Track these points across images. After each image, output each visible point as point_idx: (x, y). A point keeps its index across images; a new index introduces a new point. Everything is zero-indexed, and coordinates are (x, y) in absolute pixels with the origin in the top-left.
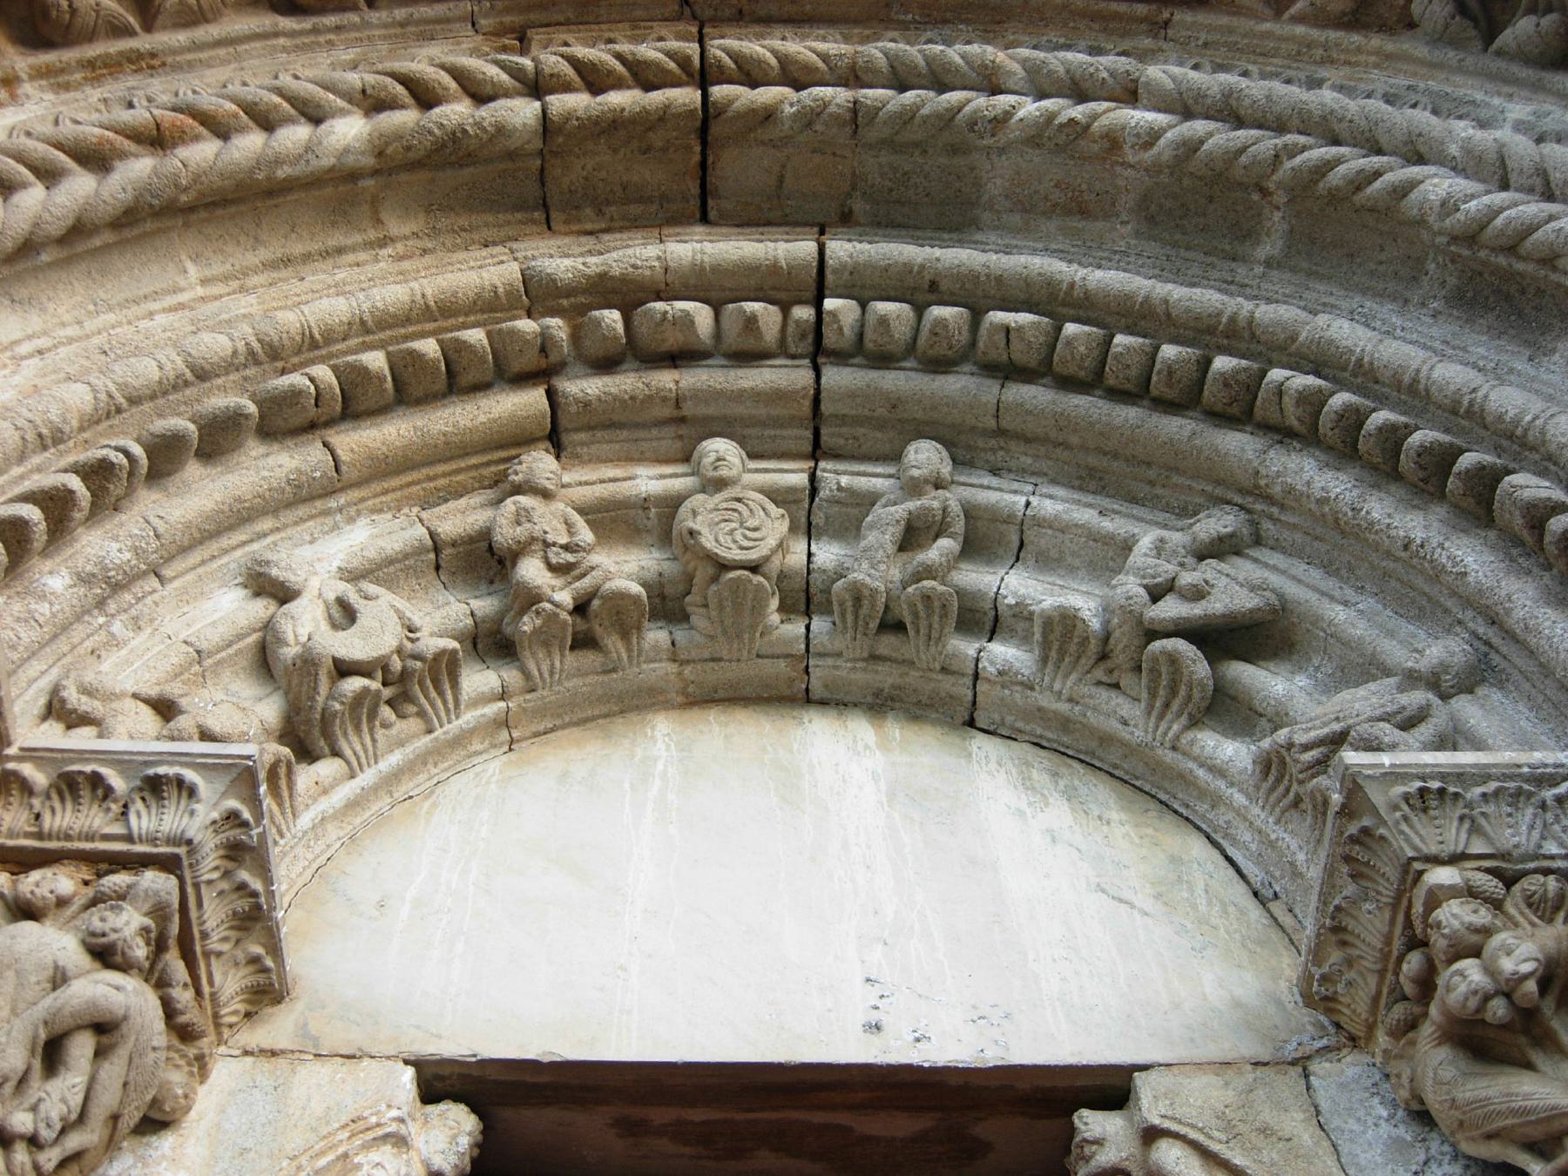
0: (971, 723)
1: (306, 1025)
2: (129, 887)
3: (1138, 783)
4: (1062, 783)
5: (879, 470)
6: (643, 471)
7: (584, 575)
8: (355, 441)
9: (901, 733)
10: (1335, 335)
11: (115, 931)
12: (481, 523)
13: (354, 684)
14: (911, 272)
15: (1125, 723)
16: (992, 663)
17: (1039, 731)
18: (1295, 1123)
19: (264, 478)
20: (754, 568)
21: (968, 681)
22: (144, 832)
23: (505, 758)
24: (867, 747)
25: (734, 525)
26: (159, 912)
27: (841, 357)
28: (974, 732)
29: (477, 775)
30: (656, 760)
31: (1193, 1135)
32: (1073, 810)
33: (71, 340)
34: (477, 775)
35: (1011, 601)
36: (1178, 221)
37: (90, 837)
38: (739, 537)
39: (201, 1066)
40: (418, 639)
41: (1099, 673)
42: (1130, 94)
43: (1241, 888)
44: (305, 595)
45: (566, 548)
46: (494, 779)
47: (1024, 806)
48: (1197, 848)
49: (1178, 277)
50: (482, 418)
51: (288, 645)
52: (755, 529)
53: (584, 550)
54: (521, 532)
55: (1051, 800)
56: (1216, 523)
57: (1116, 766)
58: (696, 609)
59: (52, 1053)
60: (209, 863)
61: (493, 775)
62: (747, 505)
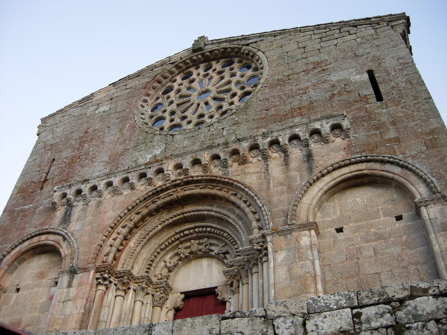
6: (188, 243)
8: (168, 249)
13: (172, 268)
18: (225, 289)
26: (164, 290)
39: (169, 296)
42: (212, 211)
49: (219, 225)
59: (160, 299)
60: (165, 286)
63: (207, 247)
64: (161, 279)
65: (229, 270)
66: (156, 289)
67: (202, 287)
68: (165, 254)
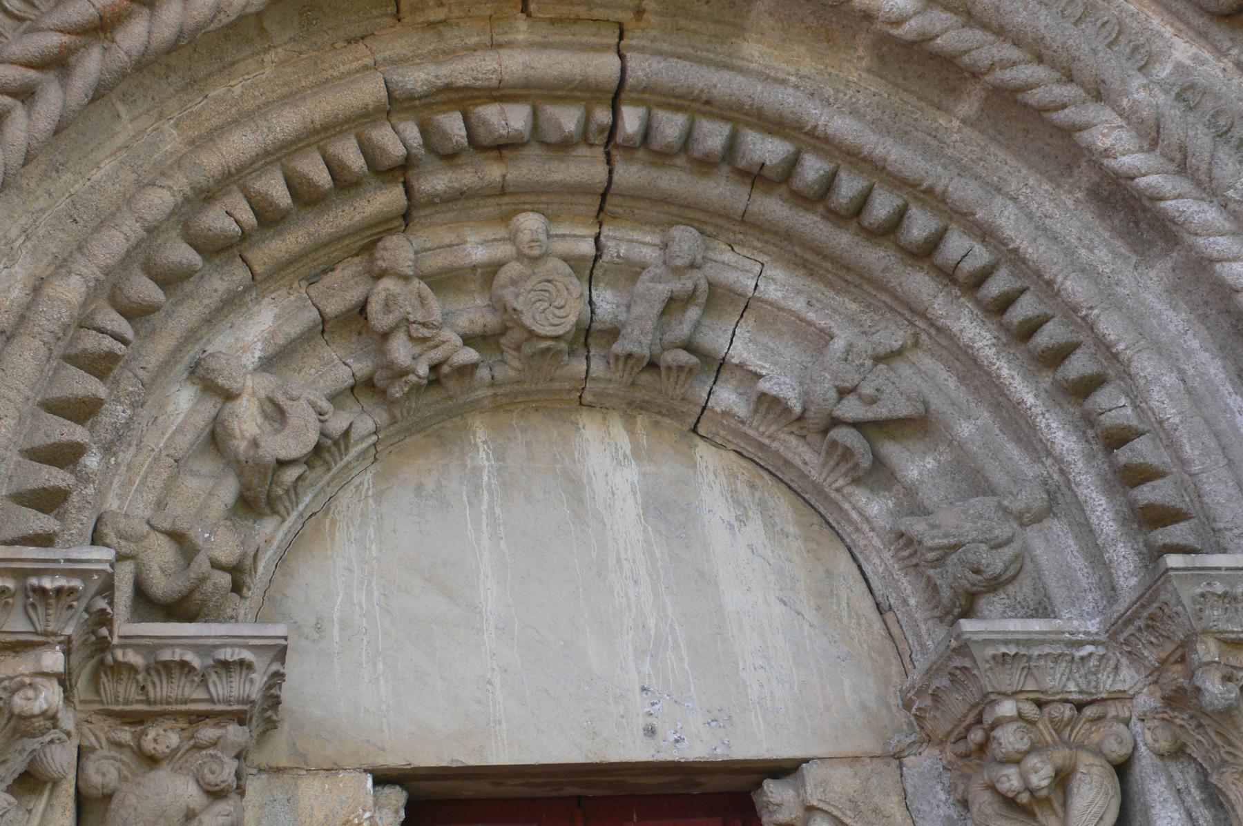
0: (694, 430)
1: (294, 744)
2: (219, 738)
3: (807, 496)
4: (758, 495)
5: (648, 239)
7: (436, 346)
9: (647, 440)
10: (1004, 224)
11: (223, 782)
12: (355, 299)
13: (291, 475)
14: (692, 93)
15: (806, 463)
16: (717, 403)
17: (742, 445)
19: (206, 306)
20: (557, 338)
21: (699, 410)
22: (221, 697)
23: (372, 469)
24: (625, 456)
25: (546, 304)
27: (629, 148)
28: (697, 440)
29: (357, 487)
30: (481, 469)
31: (836, 813)
32: (764, 523)
33: (43, 211)
34: (357, 487)
35: (735, 361)
36: (902, 65)
37: (185, 702)
38: (550, 316)
40: (326, 421)
41: (794, 428)
43: (869, 601)
44: (245, 397)
45: (424, 325)
46: (370, 493)
47: (733, 521)
48: (844, 564)
50: (357, 218)
51: (235, 438)
52: (562, 307)
53: (437, 328)
54: (390, 320)
55: (750, 514)
56: (893, 336)
57: (792, 481)
58: (510, 351)
61: (368, 488)
62: (555, 286)
63: (682, 327)
64: (177, 609)
65: (1028, 643)
66: (138, 720)
67: (637, 751)
68: (231, 304)
